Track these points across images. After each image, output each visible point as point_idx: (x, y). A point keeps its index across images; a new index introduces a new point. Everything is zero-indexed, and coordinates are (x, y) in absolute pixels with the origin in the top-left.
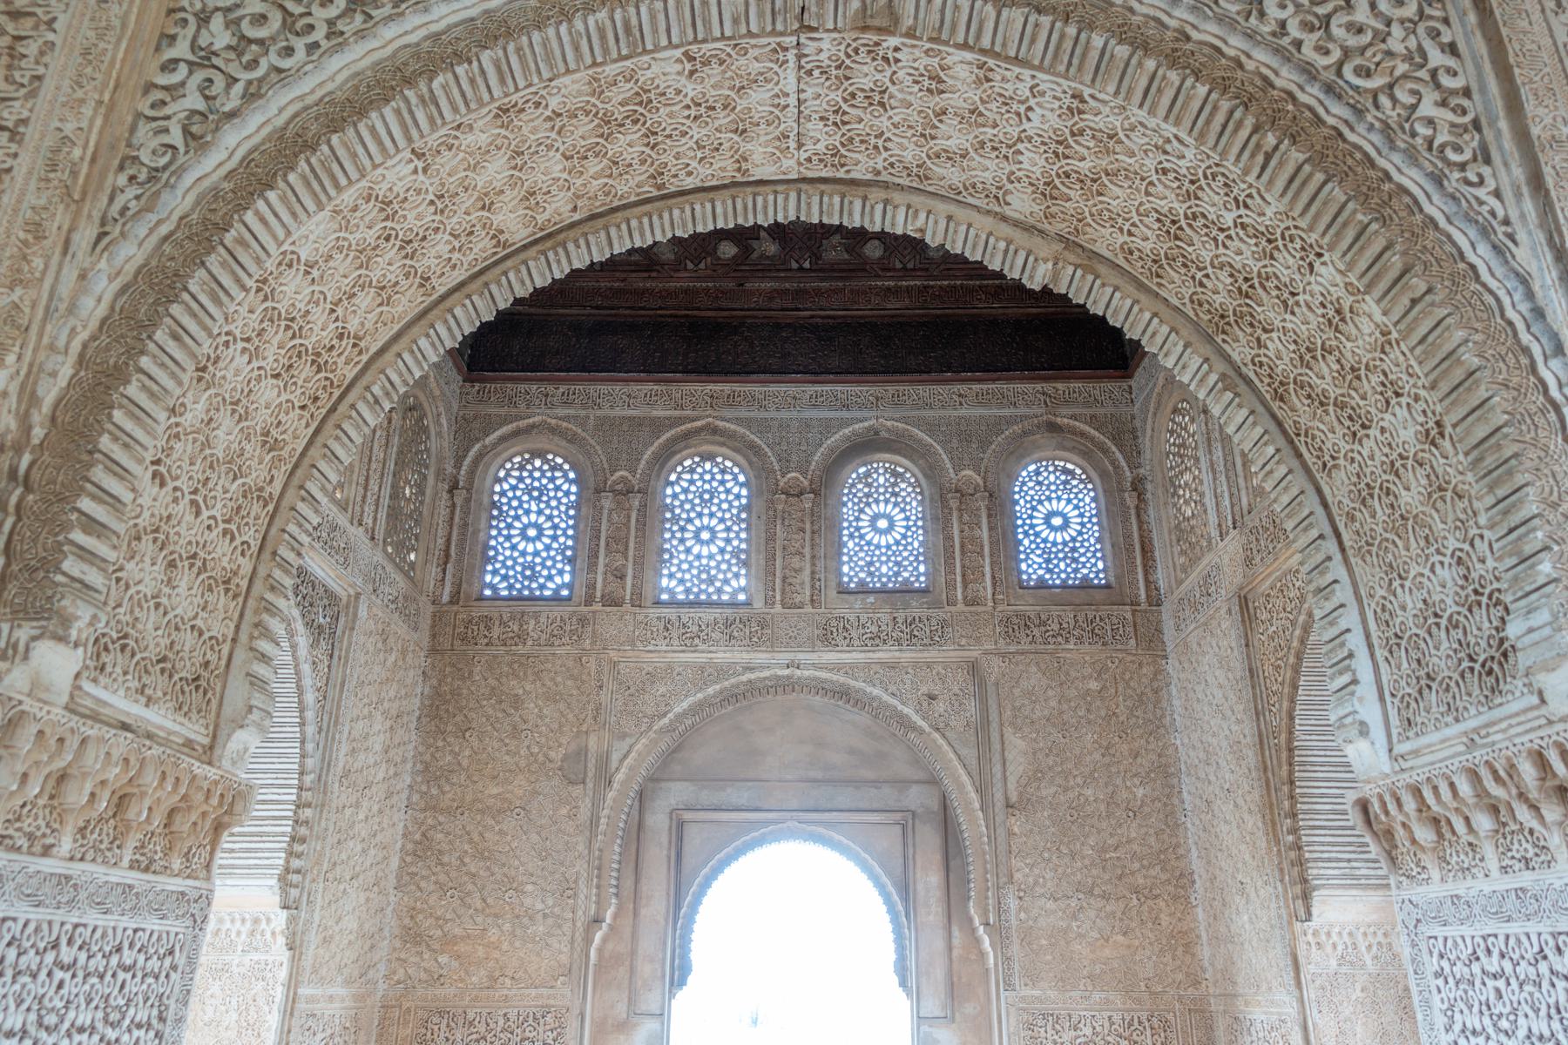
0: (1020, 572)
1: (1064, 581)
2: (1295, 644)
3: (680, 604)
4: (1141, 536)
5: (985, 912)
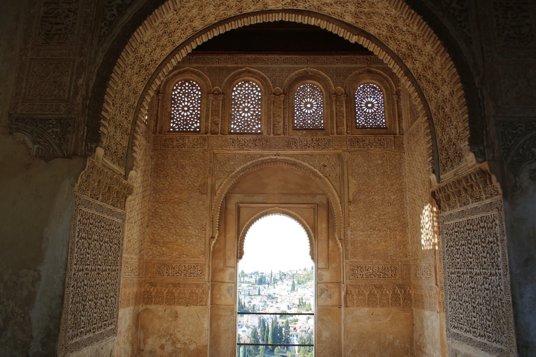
0: (357, 123)
1: (371, 126)
3: (238, 134)
4: (398, 111)
5: (340, 235)
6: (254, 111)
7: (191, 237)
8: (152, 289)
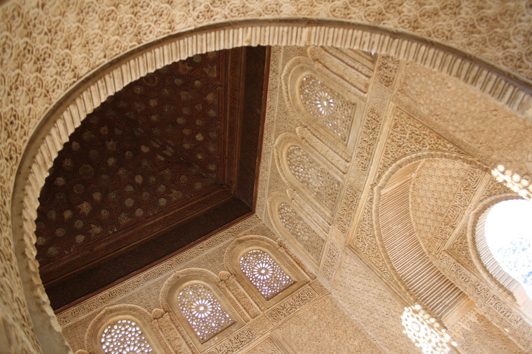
0: (263, 296)
2: (379, 243)
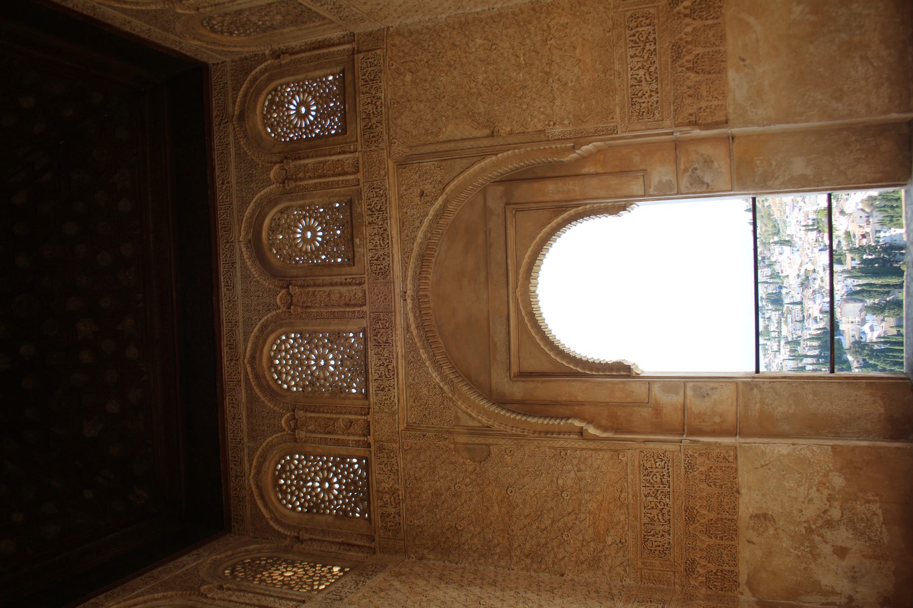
4: (310, 50)
6: (324, 346)
7: (580, 480)
8: (701, 571)
